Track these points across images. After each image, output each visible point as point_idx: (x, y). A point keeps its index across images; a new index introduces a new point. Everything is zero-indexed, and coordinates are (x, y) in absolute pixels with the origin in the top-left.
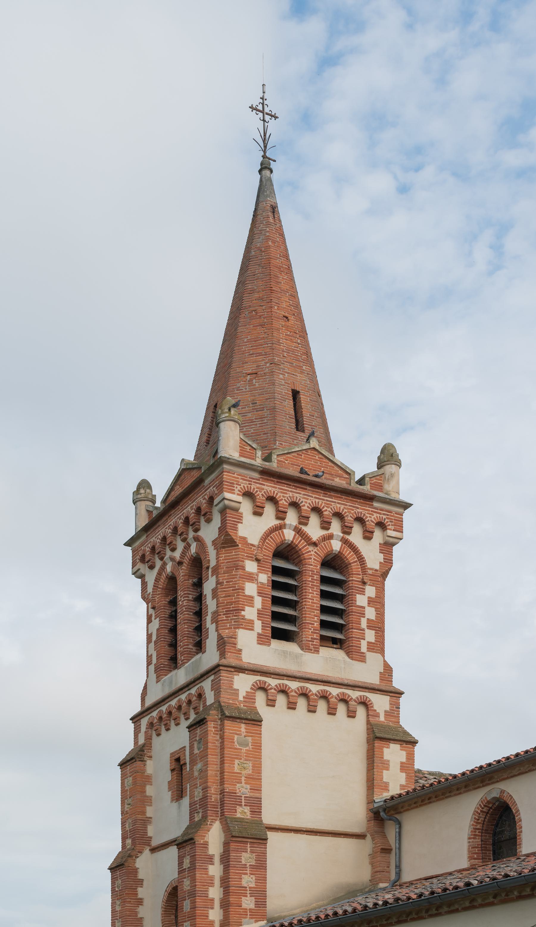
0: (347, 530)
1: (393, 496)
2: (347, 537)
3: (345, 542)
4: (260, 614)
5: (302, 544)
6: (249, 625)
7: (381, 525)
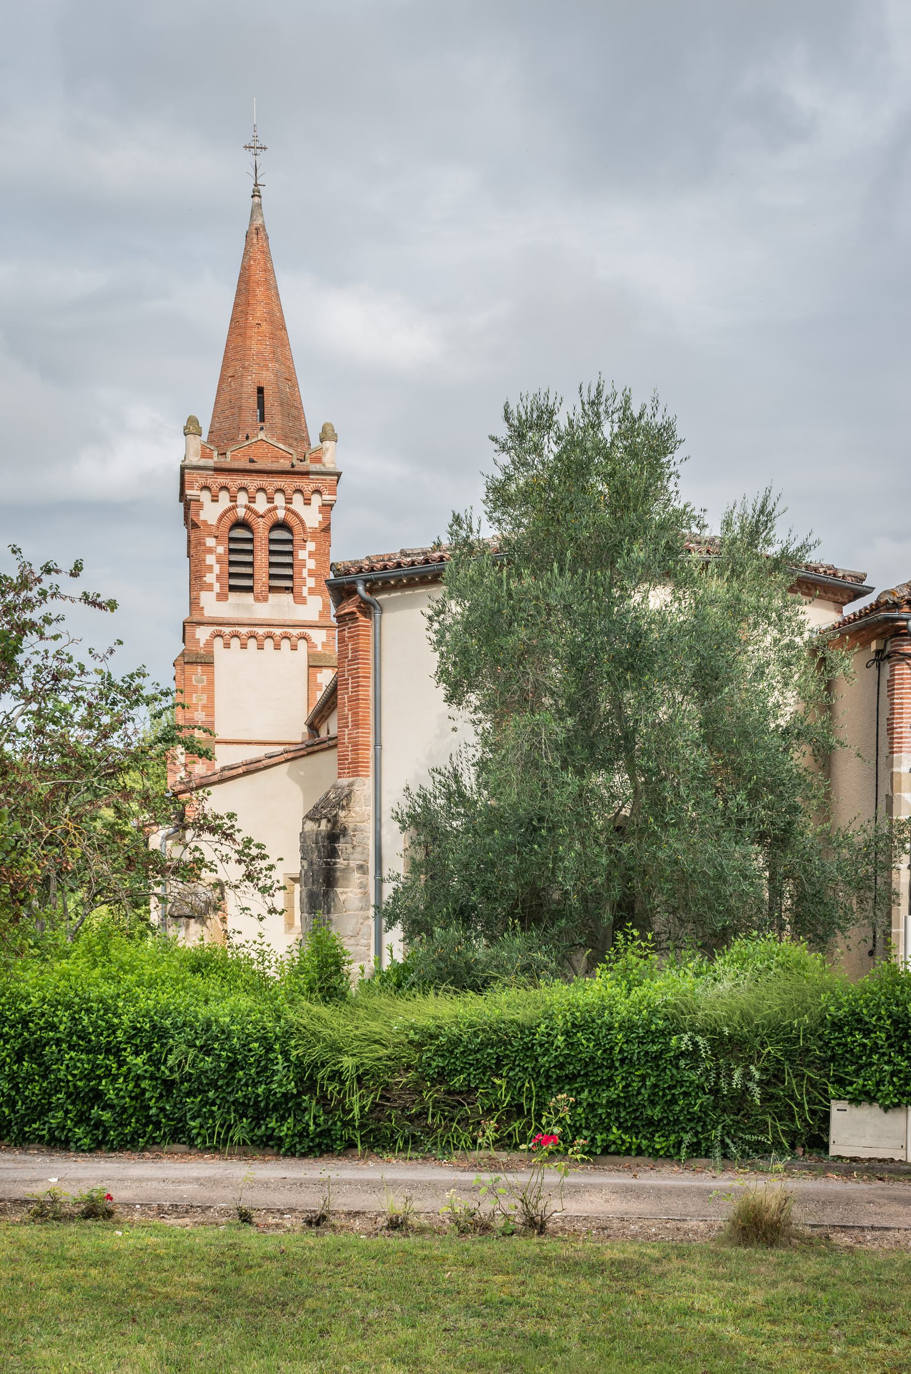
0: (289, 501)
1: (330, 467)
2: (289, 506)
3: (288, 510)
4: (218, 578)
5: (251, 518)
6: (210, 587)
7: (317, 491)
